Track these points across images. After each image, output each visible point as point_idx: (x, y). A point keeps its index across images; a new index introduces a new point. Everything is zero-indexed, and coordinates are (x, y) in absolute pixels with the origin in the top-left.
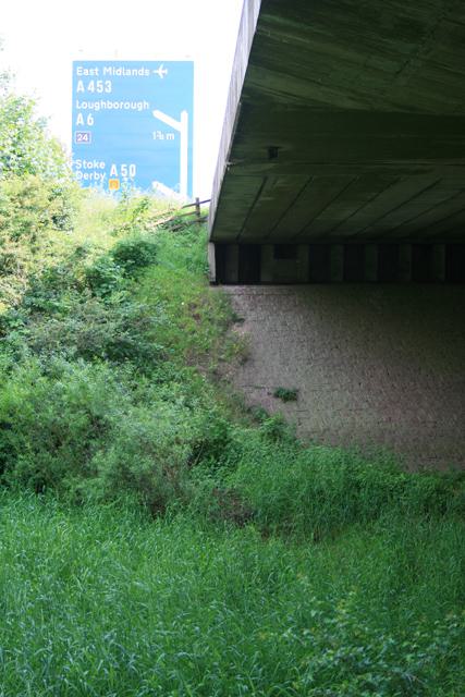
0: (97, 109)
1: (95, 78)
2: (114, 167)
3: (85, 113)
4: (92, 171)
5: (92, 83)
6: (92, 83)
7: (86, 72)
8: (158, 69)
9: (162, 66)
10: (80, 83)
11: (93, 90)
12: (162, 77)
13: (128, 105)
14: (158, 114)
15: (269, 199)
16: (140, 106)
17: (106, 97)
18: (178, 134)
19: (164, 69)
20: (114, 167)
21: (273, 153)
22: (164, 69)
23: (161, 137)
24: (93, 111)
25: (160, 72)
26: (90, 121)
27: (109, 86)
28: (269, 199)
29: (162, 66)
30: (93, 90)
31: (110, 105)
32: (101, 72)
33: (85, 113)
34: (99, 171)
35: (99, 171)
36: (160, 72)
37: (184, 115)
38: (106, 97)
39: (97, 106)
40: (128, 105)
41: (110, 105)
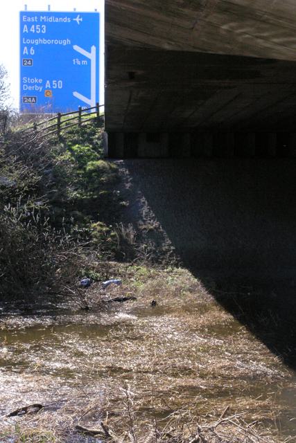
0: (37, 43)
1: (35, 23)
2: (48, 82)
3: (29, 46)
4: (34, 84)
5: (33, 26)
6: (33, 26)
7: (29, 20)
8: (76, 18)
9: (79, 16)
10: (25, 26)
11: (33, 31)
12: (78, 23)
13: (56, 42)
14: (76, 48)
15: (137, 104)
16: (65, 42)
17: (41, 36)
18: (89, 61)
19: (80, 18)
20: (48, 82)
21: (132, 76)
22: (80, 18)
23: (79, 63)
24: (34, 45)
25: (77, 20)
26: (32, 52)
27: (44, 29)
28: (137, 104)
29: (79, 16)
30: (33, 31)
31: (45, 42)
32: (39, 19)
33: (29, 46)
34: (39, 85)
35: (39, 85)
36: (77, 20)
37: (93, 48)
38: (41, 36)
39: (37, 42)
40: (56, 42)
41: (45, 42)
